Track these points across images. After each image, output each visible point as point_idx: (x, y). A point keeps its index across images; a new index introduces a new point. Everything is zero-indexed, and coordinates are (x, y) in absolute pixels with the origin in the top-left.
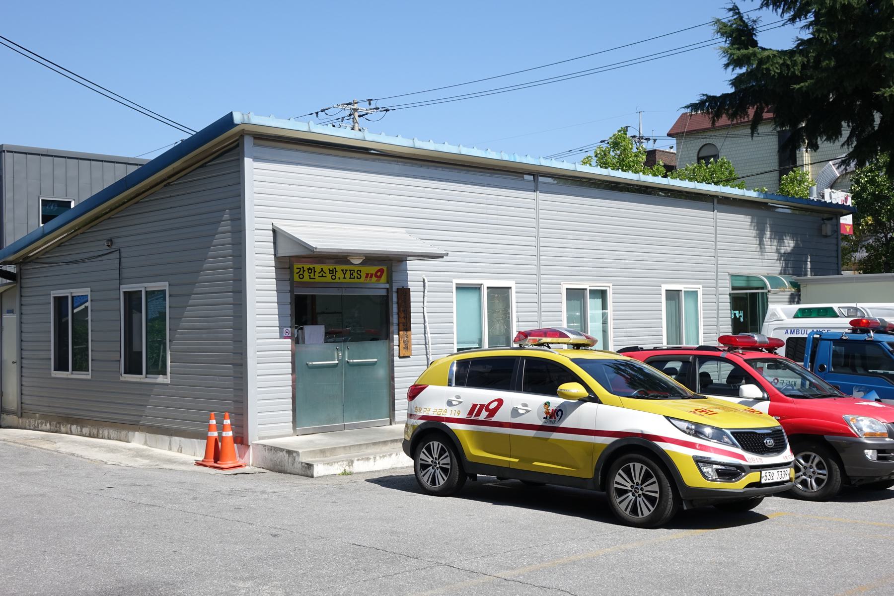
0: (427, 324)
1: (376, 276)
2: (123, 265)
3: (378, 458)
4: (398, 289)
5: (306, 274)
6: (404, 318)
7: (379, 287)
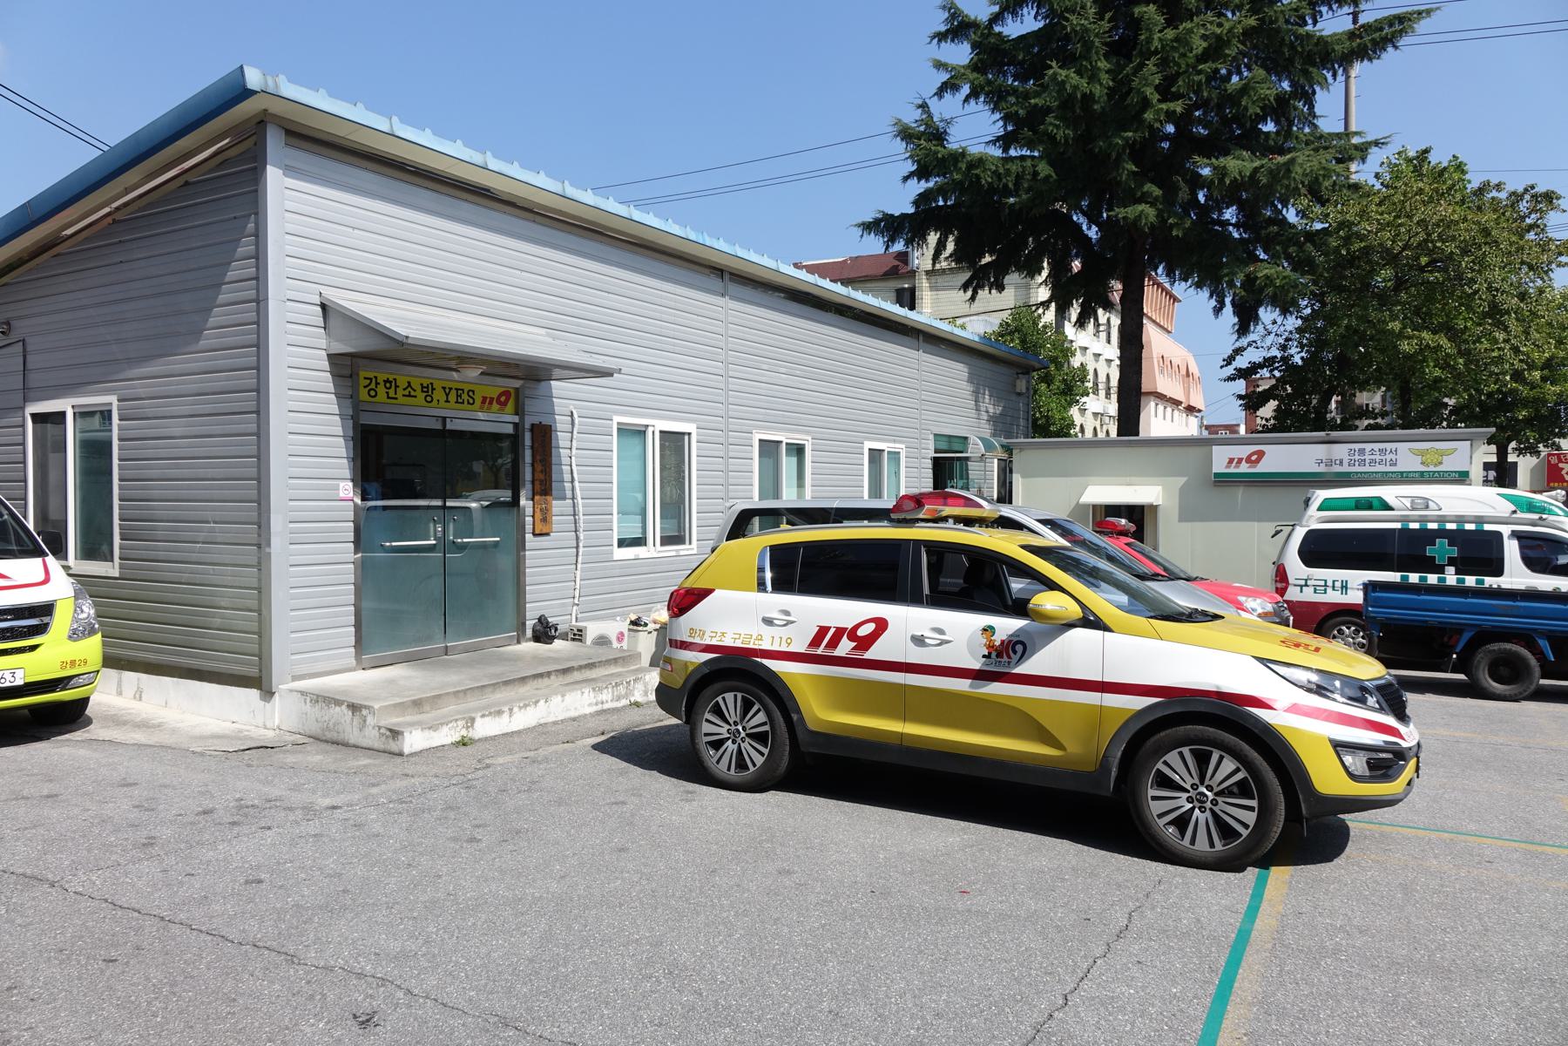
0: (577, 484)
1: (499, 402)
2: (29, 366)
3: (516, 709)
4: (533, 425)
5: (381, 390)
6: (542, 471)
7: (499, 422)
